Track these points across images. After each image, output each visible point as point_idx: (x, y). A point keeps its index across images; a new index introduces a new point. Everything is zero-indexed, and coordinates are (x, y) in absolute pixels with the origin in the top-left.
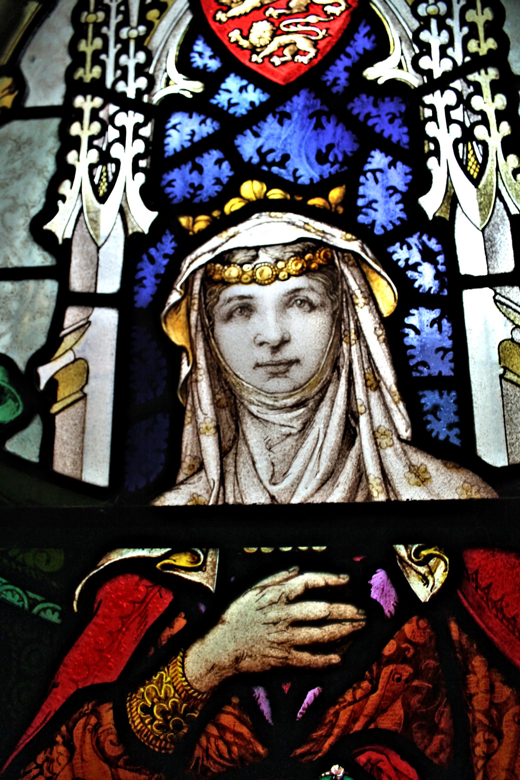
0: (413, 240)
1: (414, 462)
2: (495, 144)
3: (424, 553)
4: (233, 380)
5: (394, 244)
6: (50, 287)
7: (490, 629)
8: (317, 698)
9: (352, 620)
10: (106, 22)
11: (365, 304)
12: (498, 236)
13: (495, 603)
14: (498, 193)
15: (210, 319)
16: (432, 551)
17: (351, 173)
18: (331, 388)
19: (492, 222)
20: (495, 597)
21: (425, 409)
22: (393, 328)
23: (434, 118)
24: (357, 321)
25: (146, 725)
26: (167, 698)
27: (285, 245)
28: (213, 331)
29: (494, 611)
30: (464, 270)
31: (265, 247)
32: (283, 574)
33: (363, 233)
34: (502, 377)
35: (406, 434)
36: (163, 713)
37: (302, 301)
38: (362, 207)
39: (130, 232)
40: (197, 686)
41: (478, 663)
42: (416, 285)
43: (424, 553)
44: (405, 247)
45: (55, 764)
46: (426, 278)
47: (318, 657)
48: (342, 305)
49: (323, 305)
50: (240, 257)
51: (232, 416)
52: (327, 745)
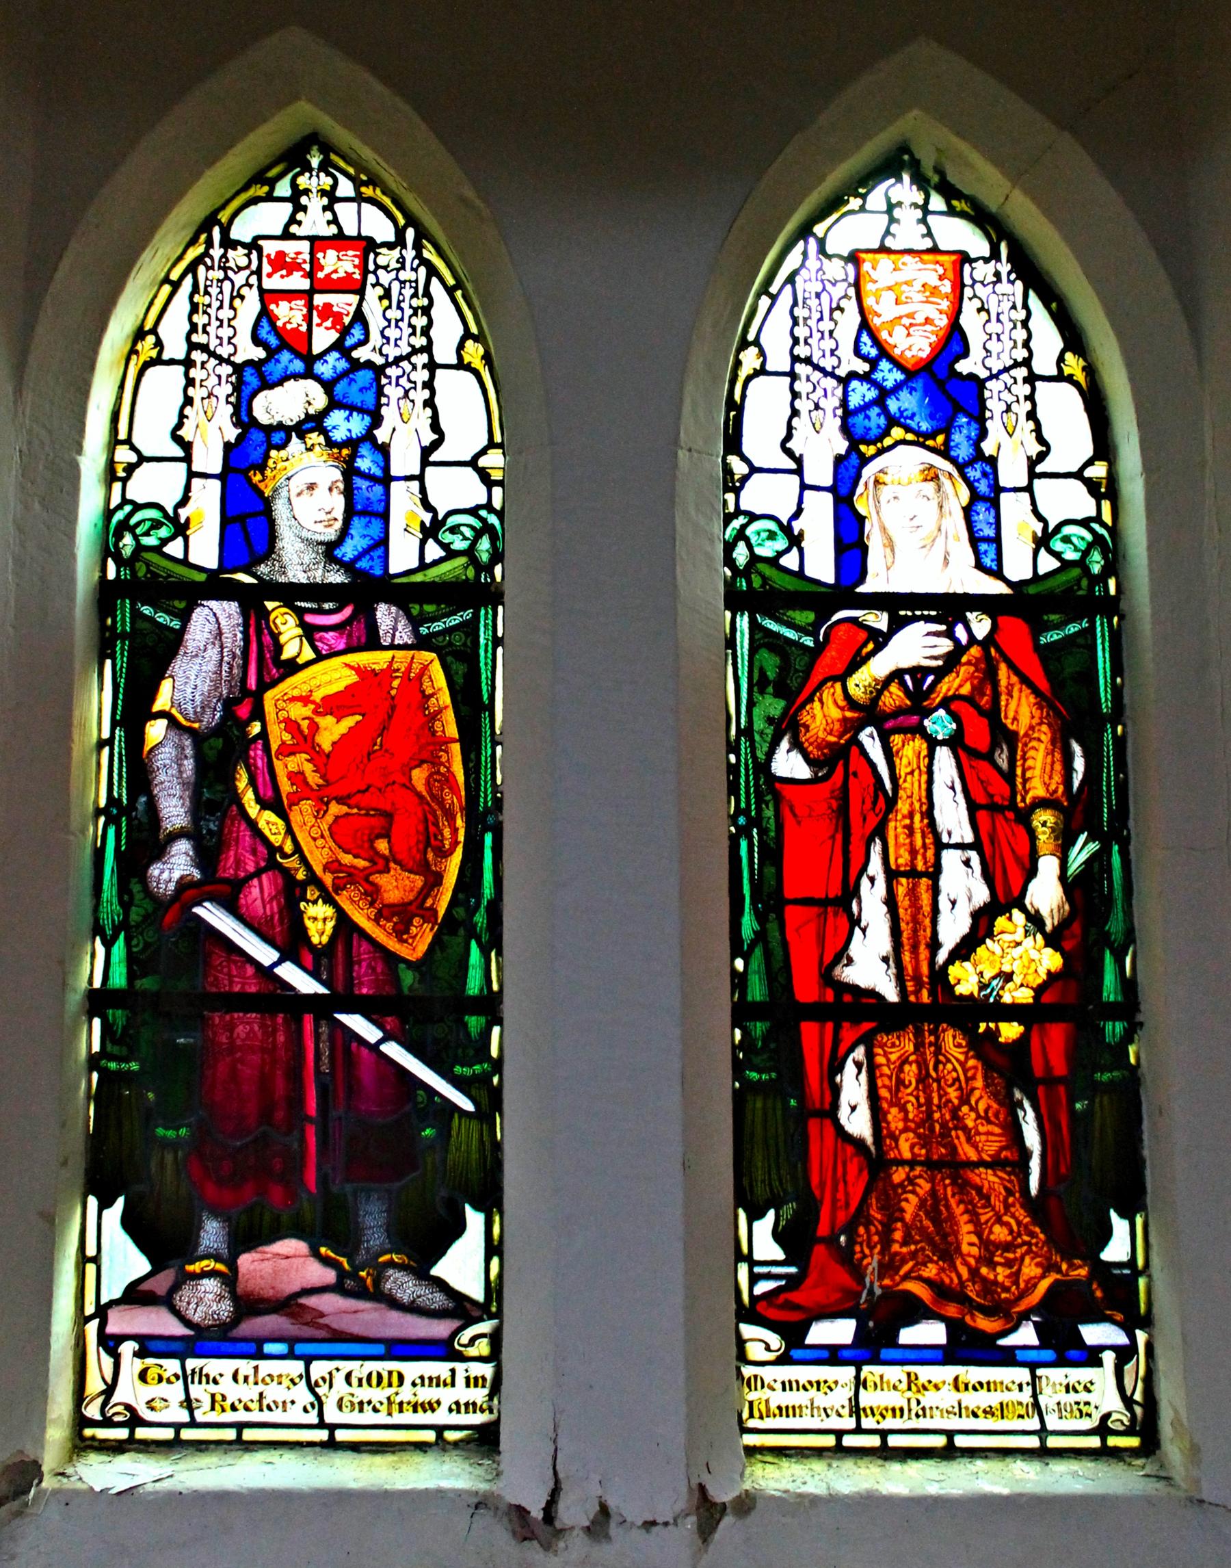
10: (209, 306)
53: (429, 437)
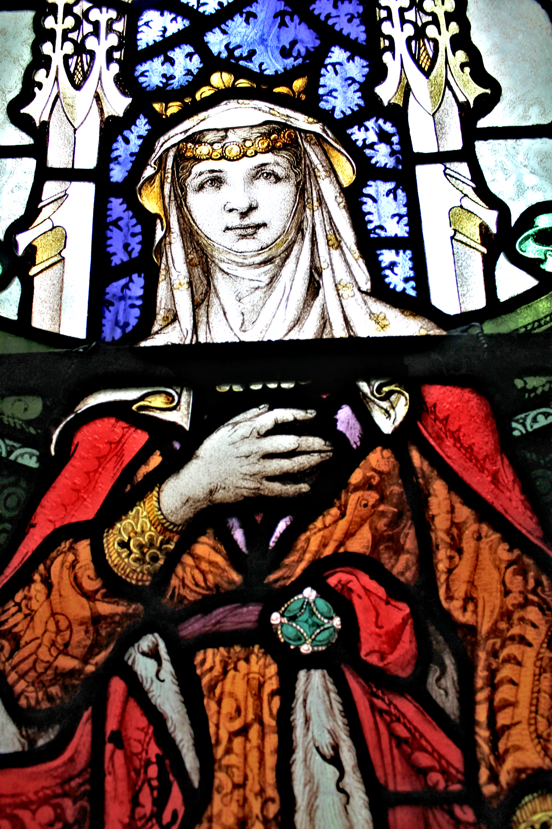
0: (370, 124)
1: (374, 311)
2: (444, 41)
3: (386, 389)
4: (204, 241)
5: (352, 127)
6: (29, 165)
7: (449, 457)
8: (288, 528)
9: (320, 452)
11: (326, 177)
12: (447, 120)
13: (452, 433)
14: (447, 83)
15: (182, 190)
16: (393, 387)
17: (313, 65)
18: (296, 248)
19: (442, 108)
20: (453, 428)
21: (383, 265)
22: (353, 198)
23: (389, 18)
24: (319, 191)
25: (123, 559)
26: (143, 532)
27: (252, 127)
28: (185, 200)
29: (452, 441)
30: (416, 148)
31: (233, 128)
32: (254, 411)
33: (325, 117)
34: (452, 238)
35: (366, 286)
36: (141, 547)
37: (268, 174)
38: (323, 95)
39: (106, 116)
40: (173, 519)
41: (439, 487)
42: (373, 161)
43: (386, 389)
44: (363, 129)
45: (34, 601)
46: (382, 156)
47: (288, 487)
48: (305, 177)
49: (287, 177)
50: (210, 137)
51: (204, 272)
52: (299, 571)
53: (471, 91)
